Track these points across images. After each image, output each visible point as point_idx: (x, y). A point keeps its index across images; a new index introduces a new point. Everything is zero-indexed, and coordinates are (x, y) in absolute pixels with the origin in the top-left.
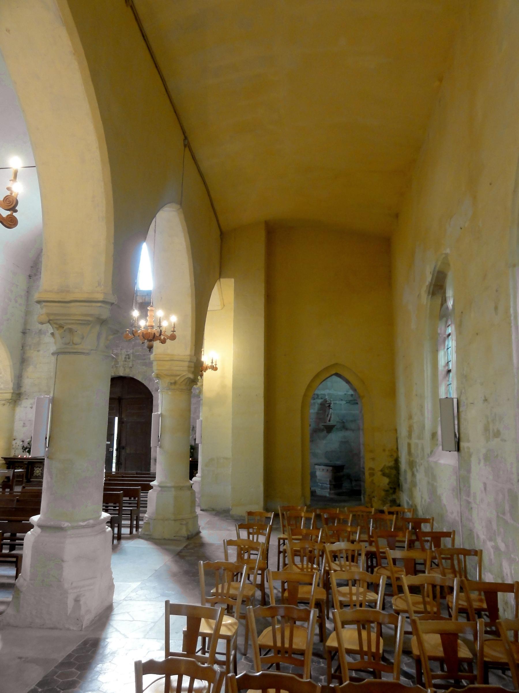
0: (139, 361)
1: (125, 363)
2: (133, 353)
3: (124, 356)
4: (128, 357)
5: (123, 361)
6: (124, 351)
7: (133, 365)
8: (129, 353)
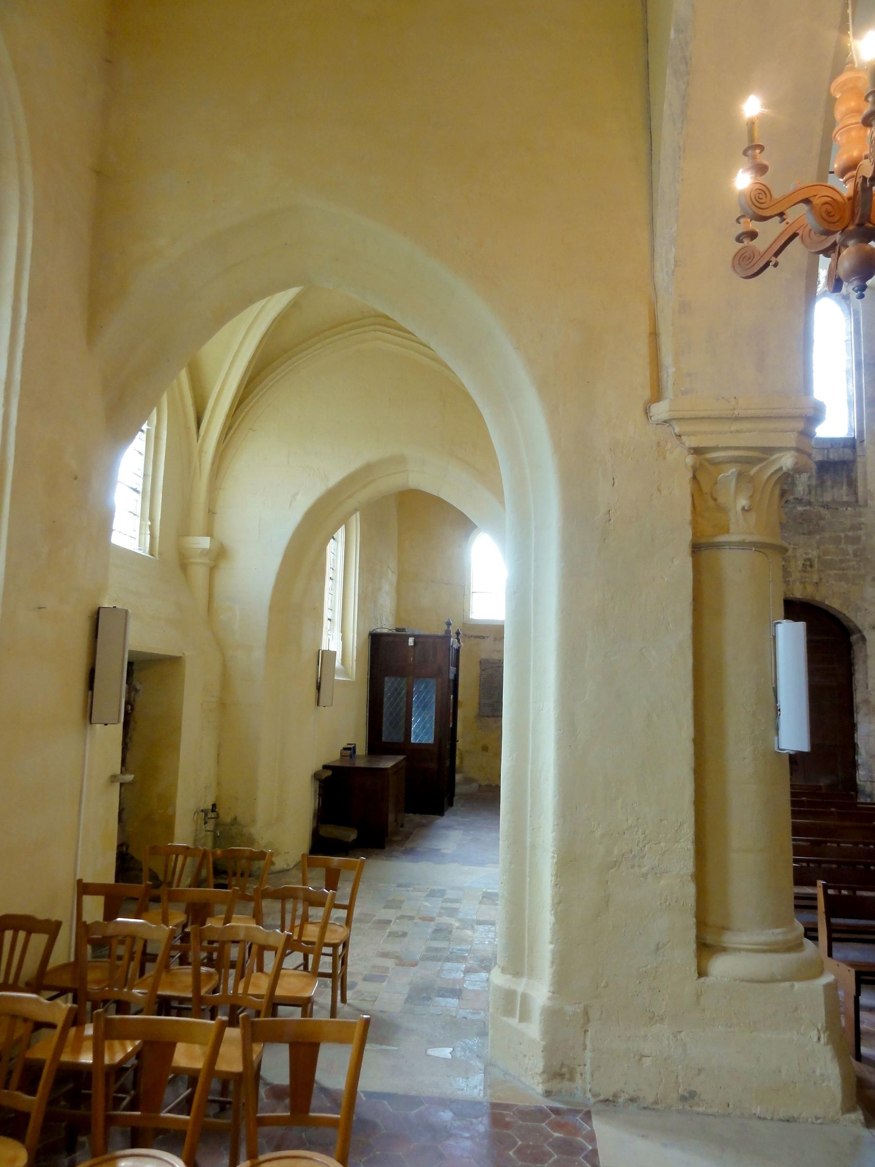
0: (832, 572)
1: (804, 574)
2: (819, 557)
3: (800, 563)
4: (809, 564)
5: (800, 571)
6: (799, 552)
7: (820, 579)
8: (810, 556)
